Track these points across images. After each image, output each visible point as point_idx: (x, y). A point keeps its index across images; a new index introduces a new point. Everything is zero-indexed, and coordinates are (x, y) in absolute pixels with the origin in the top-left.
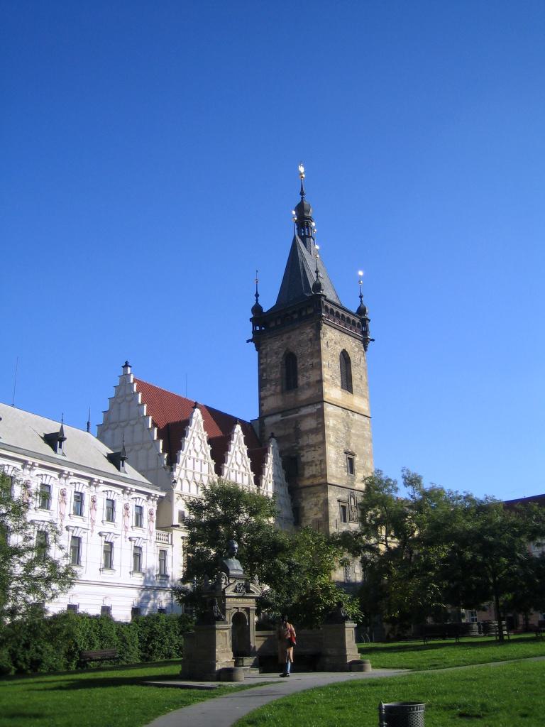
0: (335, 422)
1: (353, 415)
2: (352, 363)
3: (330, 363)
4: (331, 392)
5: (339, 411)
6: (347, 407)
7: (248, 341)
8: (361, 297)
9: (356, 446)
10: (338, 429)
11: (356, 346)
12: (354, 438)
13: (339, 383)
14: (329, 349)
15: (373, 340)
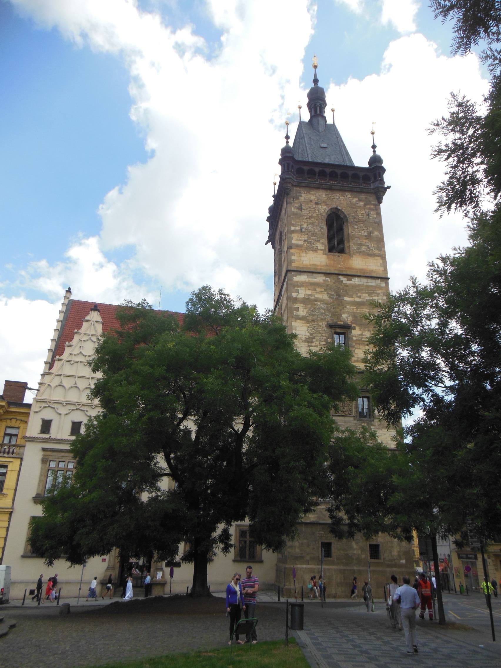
0: (309, 292)
1: (351, 280)
2: (350, 219)
3: (305, 226)
4: (303, 258)
5: (320, 279)
6: (336, 272)
7: (266, 243)
8: (374, 147)
9: (354, 316)
10: (316, 300)
11: (360, 200)
12: (349, 308)
13: (320, 246)
14: (304, 212)
15: (389, 187)
